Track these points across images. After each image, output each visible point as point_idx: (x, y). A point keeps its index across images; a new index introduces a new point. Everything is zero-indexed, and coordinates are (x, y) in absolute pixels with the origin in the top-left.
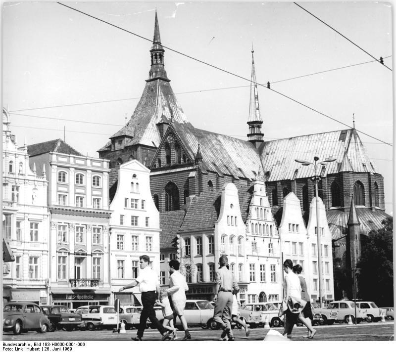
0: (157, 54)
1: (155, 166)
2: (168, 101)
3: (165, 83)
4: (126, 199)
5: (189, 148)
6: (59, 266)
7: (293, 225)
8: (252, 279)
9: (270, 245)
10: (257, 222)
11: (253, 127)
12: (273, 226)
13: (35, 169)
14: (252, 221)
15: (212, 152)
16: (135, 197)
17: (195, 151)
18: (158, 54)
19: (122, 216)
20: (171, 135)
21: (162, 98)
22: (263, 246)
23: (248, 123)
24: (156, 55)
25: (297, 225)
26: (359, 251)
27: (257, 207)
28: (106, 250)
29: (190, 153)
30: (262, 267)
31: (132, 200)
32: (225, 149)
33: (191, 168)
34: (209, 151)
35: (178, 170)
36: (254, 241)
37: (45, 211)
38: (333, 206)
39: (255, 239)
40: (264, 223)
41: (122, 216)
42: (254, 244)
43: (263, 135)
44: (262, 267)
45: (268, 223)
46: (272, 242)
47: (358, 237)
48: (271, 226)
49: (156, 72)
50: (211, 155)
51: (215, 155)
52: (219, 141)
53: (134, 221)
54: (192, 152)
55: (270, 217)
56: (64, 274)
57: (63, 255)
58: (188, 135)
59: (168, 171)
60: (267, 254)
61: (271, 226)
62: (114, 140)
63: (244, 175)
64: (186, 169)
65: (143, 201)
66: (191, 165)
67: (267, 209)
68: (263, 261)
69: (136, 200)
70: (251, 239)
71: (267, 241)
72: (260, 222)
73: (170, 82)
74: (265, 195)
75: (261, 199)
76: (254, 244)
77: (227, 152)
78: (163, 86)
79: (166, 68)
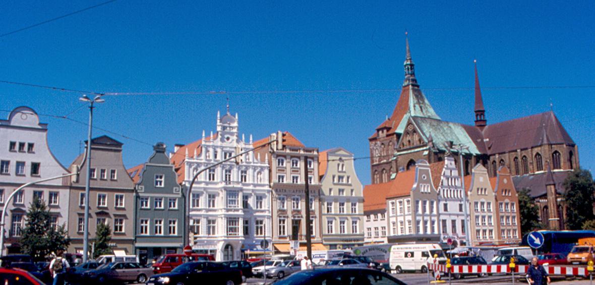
1: (400, 148)
2: (418, 100)
3: (416, 88)
4: (334, 177)
5: (424, 134)
6: (280, 227)
8: (370, 235)
9: (461, 206)
11: (477, 116)
13: (259, 157)
15: (443, 136)
16: (341, 174)
17: (428, 136)
19: (330, 190)
21: (413, 99)
22: (453, 207)
23: (476, 112)
24: (408, 68)
25: (485, 190)
26: (555, 205)
28: (317, 214)
29: (423, 137)
30: (454, 222)
32: (454, 133)
33: (425, 148)
34: (441, 135)
35: (413, 151)
37: (267, 188)
38: (538, 170)
41: (330, 190)
42: (445, 205)
43: (485, 121)
44: (454, 222)
49: (409, 80)
50: (442, 137)
51: (445, 138)
52: (450, 127)
53: (341, 191)
54: (426, 136)
56: (284, 232)
57: (282, 218)
58: (423, 124)
59: (409, 151)
60: (458, 212)
62: (378, 130)
63: (469, 151)
64: (421, 149)
65: (348, 178)
66: (426, 145)
68: (453, 218)
71: (459, 203)
76: (445, 205)
77: (455, 135)
78: (414, 90)
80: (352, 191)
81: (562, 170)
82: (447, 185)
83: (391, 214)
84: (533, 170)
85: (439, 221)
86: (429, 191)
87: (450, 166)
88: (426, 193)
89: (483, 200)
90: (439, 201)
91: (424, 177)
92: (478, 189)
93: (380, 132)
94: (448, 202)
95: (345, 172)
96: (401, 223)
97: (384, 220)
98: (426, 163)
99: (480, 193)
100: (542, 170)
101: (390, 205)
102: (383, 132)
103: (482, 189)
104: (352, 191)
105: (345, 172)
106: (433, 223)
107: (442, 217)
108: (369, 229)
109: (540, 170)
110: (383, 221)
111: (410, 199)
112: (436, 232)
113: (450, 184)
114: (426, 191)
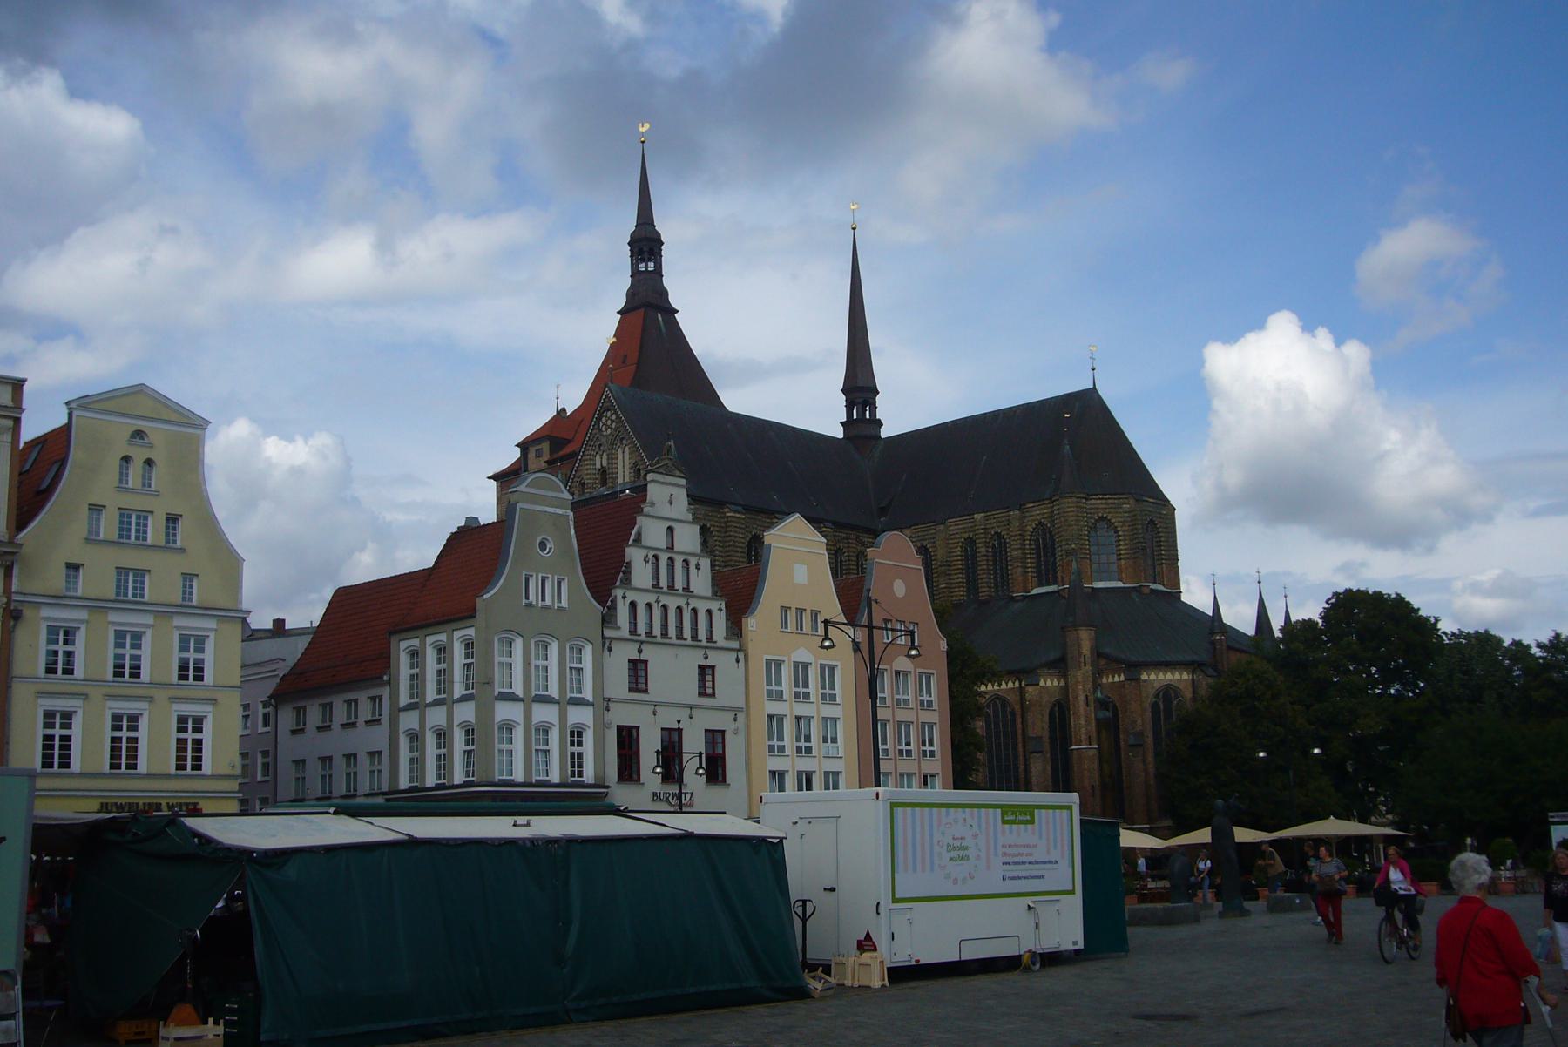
0: (646, 245)
7: (801, 611)
9: (705, 671)
10: (651, 598)
11: (849, 407)
12: (716, 614)
14: (631, 596)
18: (645, 249)
20: (609, 414)
27: (651, 554)
31: (125, 513)
36: (636, 656)
38: (1041, 585)
39: (640, 651)
40: (673, 603)
41: (73, 567)
42: (638, 670)
45: (694, 603)
46: (710, 662)
47: (1088, 660)
48: (709, 612)
55: (701, 581)
61: (709, 612)
62: (524, 446)
65: (172, 520)
67: (693, 561)
69: (143, 515)
70: (628, 651)
71: (696, 658)
72: (664, 600)
73: (676, 315)
74: (690, 517)
75: (670, 529)
76: (638, 670)
79: (666, 283)
80: (188, 578)
81: (1120, 584)
82: (648, 584)
83: (404, 699)
84: (1025, 581)
85: (601, 726)
86: (564, 603)
87: (666, 511)
88: (545, 608)
89: (803, 655)
90: (606, 644)
91: (543, 545)
92: (785, 610)
93: (532, 454)
94: (649, 653)
95: (157, 494)
96: (469, 731)
97: (378, 721)
98: (562, 492)
99: (791, 626)
100: (1055, 583)
101: (404, 659)
102: (539, 454)
103: (801, 611)
104: (188, 578)
105: (157, 494)
106: (576, 736)
107: (622, 715)
108: (300, 763)
109: (1048, 584)
110: (375, 728)
111: (471, 632)
112: (589, 775)
113: (664, 582)
114: (548, 602)
